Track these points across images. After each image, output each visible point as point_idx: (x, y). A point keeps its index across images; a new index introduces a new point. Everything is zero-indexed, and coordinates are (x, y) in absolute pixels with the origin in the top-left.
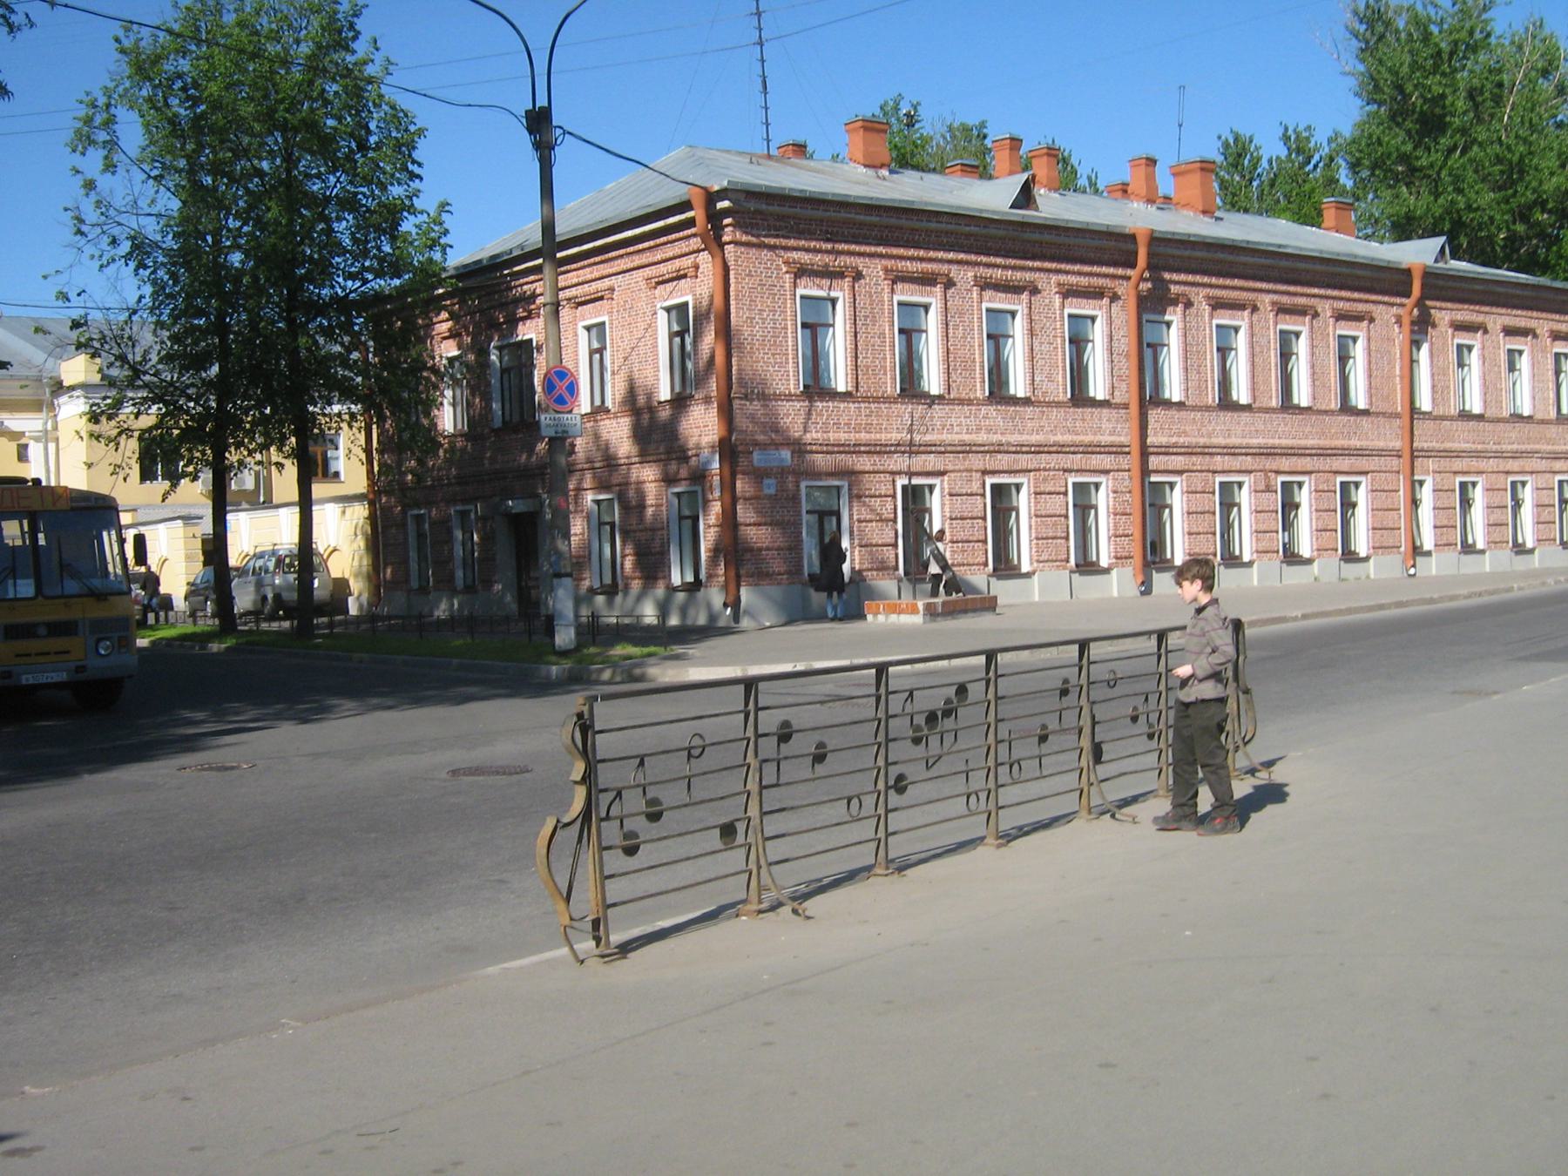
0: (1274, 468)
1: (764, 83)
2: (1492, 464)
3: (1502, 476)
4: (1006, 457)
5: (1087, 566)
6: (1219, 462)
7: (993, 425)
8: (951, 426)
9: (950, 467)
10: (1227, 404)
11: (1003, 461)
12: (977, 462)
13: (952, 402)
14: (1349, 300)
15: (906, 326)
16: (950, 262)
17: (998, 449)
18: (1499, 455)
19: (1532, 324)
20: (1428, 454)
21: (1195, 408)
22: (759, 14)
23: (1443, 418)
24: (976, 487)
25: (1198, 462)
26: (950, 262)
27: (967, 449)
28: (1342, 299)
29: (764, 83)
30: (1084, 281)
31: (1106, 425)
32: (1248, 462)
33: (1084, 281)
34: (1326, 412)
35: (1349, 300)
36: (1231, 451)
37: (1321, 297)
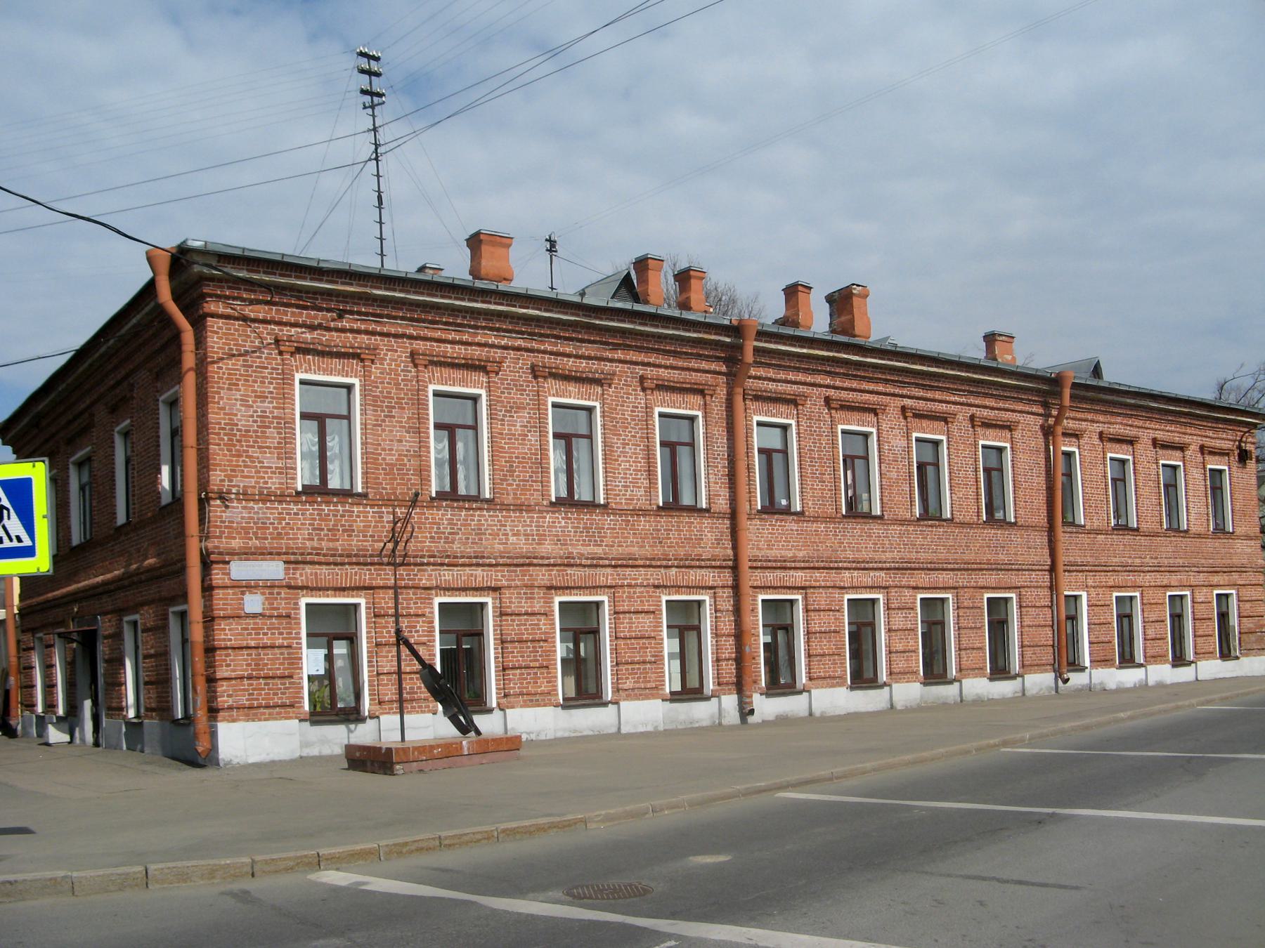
1: (380, 198)
8: (512, 534)
9: (505, 583)
10: (855, 512)
11: (575, 574)
12: (542, 576)
13: (505, 507)
15: (447, 420)
16: (505, 348)
17: (568, 563)
18: (1157, 570)
21: (816, 519)
22: (375, 130)
23: (1098, 532)
24: (538, 606)
26: (505, 348)
27: (527, 562)
29: (380, 198)
30: (675, 375)
33: (675, 375)
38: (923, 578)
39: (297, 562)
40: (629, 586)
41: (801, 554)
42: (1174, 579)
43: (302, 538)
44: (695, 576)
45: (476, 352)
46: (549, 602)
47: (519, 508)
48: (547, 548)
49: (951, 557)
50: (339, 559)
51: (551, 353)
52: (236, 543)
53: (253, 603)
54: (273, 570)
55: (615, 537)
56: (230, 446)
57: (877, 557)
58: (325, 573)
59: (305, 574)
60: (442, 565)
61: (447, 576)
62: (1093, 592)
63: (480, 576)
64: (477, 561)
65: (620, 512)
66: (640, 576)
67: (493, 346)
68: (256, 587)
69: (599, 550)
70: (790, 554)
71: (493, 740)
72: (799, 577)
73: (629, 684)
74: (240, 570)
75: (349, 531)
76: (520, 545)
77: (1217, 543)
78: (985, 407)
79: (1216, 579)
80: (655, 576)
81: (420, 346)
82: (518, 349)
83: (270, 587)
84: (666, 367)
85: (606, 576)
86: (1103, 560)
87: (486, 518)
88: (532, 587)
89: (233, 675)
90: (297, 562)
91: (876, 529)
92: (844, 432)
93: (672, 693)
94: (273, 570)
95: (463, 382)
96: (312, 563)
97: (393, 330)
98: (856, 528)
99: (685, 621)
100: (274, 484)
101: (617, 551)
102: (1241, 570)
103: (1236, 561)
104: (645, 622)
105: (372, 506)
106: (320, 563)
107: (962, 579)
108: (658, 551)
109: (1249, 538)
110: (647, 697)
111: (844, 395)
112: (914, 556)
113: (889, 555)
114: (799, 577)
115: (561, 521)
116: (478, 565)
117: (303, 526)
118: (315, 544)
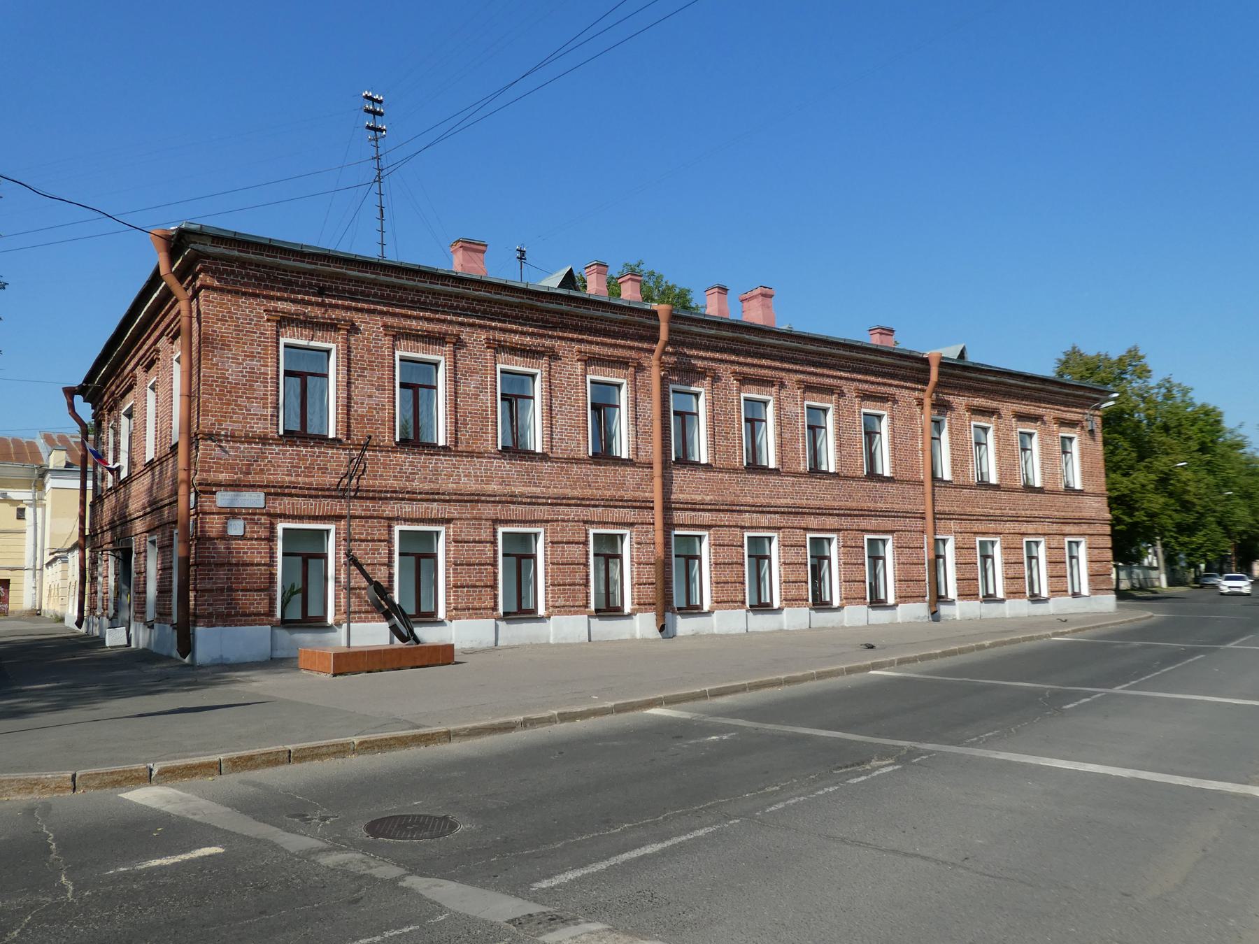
0: (803, 525)
2: (1009, 527)
3: (859, 534)
4: (520, 507)
5: (609, 609)
6: (747, 519)
7: (505, 476)
8: (463, 476)
9: (456, 515)
11: (517, 511)
12: (489, 511)
13: (459, 454)
14: (873, 383)
16: (461, 324)
17: (512, 500)
18: (1016, 519)
19: (1041, 411)
20: (948, 516)
21: (721, 470)
23: (963, 487)
24: (485, 534)
25: (725, 518)
26: (461, 324)
27: (475, 499)
28: (866, 382)
31: (630, 482)
32: (777, 520)
34: (853, 478)
35: (873, 383)
36: (761, 509)
37: (847, 379)
38: (813, 522)
39: (276, 494)
40: (563, 521)
41: (708, 498)
42: (1030, 528)
43: (281, 476)
44: (618, 514)
45: (436, 327)
46: (495, 532)
47: (471, 454)
48: (493, 487)
49: (836, 504)
50: (313, 492)
51: (501, 330)
52: (222, 477)
53: (236, 528)
54: (254, 499)
55: (550, 481)
56: (221, 395)
57: (773, 502)
58: (302, 505)
59: (281, 505)
60: (403, 499)
61: (408, 509)
62: (960, 537)
63: (435, 509)
64: (432, 496)
65: (558, 460)
66: (572, 513)
67: (451, 322)
68: (240, 514)
69: (537, 490)
70: (699, 498)
71: (369, 652)
72: (706, 517)
73: (560, 602)
74: (223, 499)
75: (324, 470)
76: (469, 485)
77: (1068, 499)
78: (866, 382)
79: (1067, 529)
80: (590, 513)
81: (390, 321)
82: (472, 325)
83: (250, 515)
84: (597, 344)
85: (542, 512)
86: (968, 510)
87: (444, 462)
88: (480, 519)
89: (214, 587)
90: (276, 494)
91: (773, 479)
92: (746, 400)
93: (597, 610)
94: (254, 499)
95: (426, 351)
96: (291, 495)
97: (366, 306)
98: (756, 478)
99: (608, 551)
100: (258, 428)
101: (552, 491)
102: (1090, 521)
103: (1085, 514)
104: (577, 550)
105: (344, 449)
106: (297, 496)
107: (845, 523)
108: (588, 492)
109: (1095, 495)
110: (576, 613)
111: (746, 369)
112: (804, 502)
113: (783, 501)
114: (706, 517)
115: (507, 467)
116: (434, 500)
117: (283, 464)
118: (293, 479)
